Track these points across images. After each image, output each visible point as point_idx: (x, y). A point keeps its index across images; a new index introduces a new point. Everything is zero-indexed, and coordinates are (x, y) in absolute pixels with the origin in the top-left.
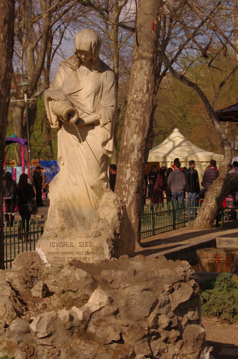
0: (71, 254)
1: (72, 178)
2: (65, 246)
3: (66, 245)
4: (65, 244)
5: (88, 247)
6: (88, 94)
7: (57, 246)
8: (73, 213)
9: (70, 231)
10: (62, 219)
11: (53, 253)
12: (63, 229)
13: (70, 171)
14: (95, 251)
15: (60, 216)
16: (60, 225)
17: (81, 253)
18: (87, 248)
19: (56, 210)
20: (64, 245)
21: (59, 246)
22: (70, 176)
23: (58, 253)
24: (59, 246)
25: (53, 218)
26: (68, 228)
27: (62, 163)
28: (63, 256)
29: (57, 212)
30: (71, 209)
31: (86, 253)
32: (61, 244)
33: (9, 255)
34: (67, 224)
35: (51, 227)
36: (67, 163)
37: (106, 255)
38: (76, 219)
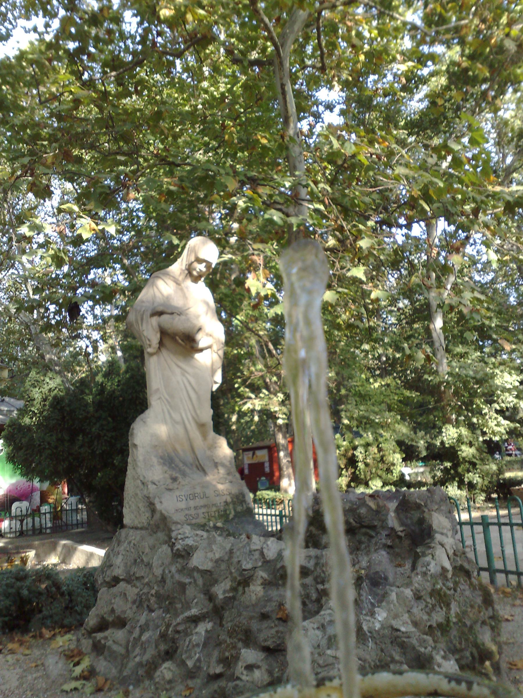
1: (173, 415)
11: (182, 510)
12: (174, 479)
13: (171, 406)
16: (167, 476)
19: (153, 457)
22: (170, 414)
23: (189, 509)
29: (155, 460)
30: (173, 454)
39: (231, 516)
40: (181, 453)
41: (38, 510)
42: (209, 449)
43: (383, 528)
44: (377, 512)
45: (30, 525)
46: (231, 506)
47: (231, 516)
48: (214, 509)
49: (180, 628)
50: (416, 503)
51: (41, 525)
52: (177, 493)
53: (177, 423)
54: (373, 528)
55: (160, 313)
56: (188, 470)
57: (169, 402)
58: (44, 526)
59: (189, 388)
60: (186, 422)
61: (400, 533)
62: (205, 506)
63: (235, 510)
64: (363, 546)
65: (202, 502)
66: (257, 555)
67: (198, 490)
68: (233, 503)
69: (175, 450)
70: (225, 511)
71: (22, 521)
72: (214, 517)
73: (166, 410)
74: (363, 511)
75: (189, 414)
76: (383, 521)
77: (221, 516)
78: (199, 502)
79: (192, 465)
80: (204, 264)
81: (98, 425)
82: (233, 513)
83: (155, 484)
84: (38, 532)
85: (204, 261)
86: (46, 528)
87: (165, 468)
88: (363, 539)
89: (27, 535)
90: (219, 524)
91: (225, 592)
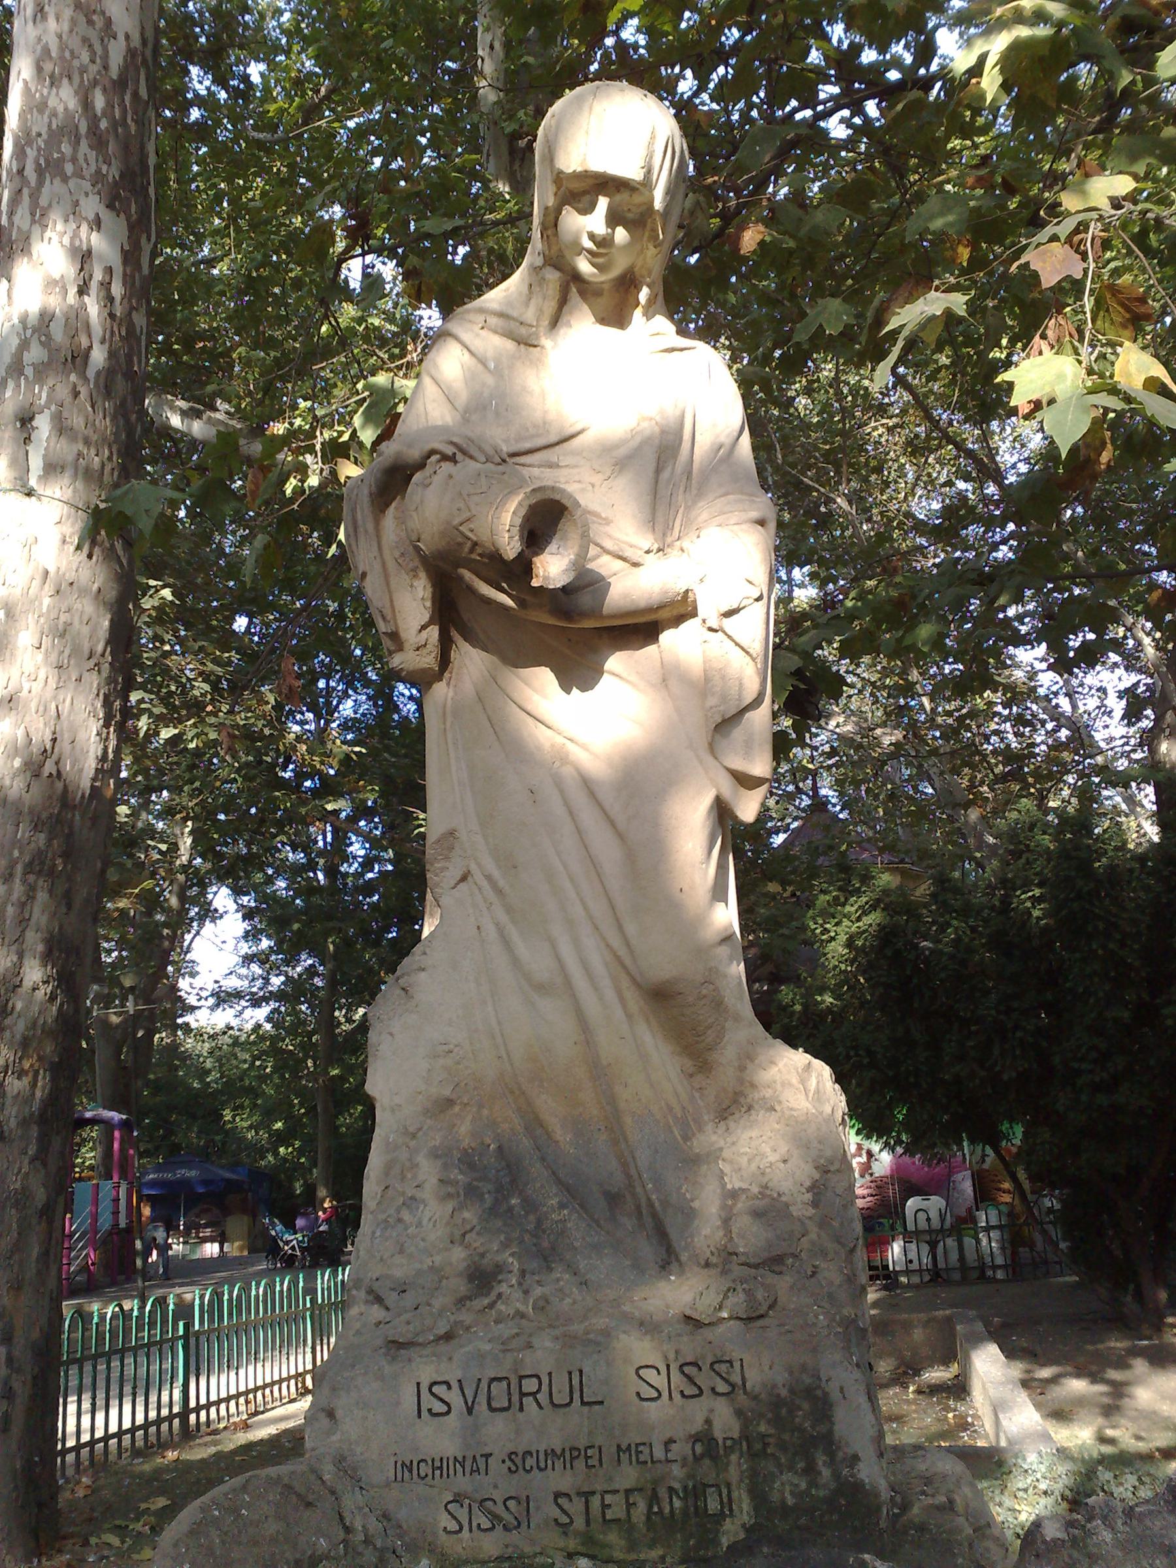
0: (580, 1464)
1: (523, 950)
2: (528, 1401)
3: (534, 1394)
4: (530, 1385)
5: (706, 1401)
7: (470, 1411)
8: (537, 1170)
9: (538, 1291)
10: (467, 1215)
11: (439, 1466)
13: (509, 910)
14: (763, 1428)
15: (449, 1196)
16: (458, 1255)
17: (659, 1453)
18: (698, 1411)
20: (522, 1395)
21: (482, 1407)
23: (476, 1463)
24: (482, 1407)
25: (406, 1216)
26: (523, 1273)
27: (455, 873)
29: (428, 1172)
31: (699, 1448)
32: (498, 1389)
34: (505, 1245)
35: (398, 1273)
36: (491, 866)
37: (856, 1458)
38: (562, 1206)
39: (731, 1532)
40: (563, 1136)
45: (954, 1256)
46: (736, 1468)
47: (731, 1532)
48: (628, 1476)
51: (980, 1257)
53: (541, 988)
57: (499, 892)
62: (571, 1455)
63: (759, 1497)
69: (534, 1124)
70: (695, 1492)
71: (933, 1245)
73: (491, 932)
75: (590, 942)
79: (613, 1199)
83: (379, 1300)
84: (975, 1274)
86: (995, 1268)
89: (948, 1282)
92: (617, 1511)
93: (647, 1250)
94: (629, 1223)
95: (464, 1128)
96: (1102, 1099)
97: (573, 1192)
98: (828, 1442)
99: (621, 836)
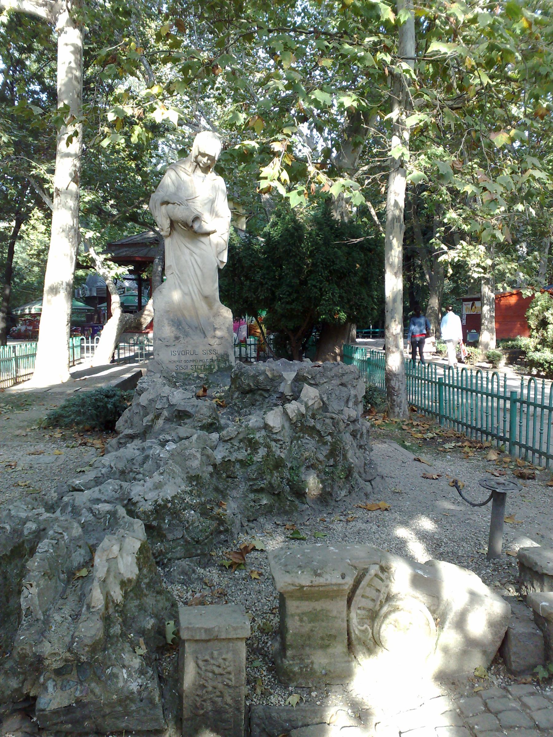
6: (206, 202)
12: (177, 338)
16: (173, 335)
23: (180, 361)
28: (186, 364)
29: (166, 322)
30: (182, 319)
33: (252, 350)
39: (215, 370)
40: (188, 318)
41: (245, 341)
42: (214, 316)
43: (275, 392)
44: (272, 380)
46: (216, 363)
48: (201, 364)
49: (122, 441)
50: (303, 376)
51: (247, 354)
52: (172, 349)
54: (267, 391)
55: (167, 203)
56: (191, 332)
58: (249, 356)
59: (196, 266)
60: (193, 294)
61: (288, 397)
63: (218, 366)
64: (258, 403)
65: (192, 358)
66: (165, 400)
67: (189, 348)
68: (218, 360)
69: (183, 315)
70: (210, 366)
72: (201, 369)
74: (261, 378)
75: (195, 288)
76: (276, 387)
77: (205, 369)
78: (189, 357)
79: (196, 328)
80: (207, 158)
81: (260, 274)
82: (217, 368)
84: (244, 360)
85: (207, 155)
86: (251, 358)
87: (173, 329)
88: (258, 397)
90: (202, 375)
91: (148, 421)
92: (199, 367)
93: (202, 336)
94: (198, 331)
95: (171, 315)
96: (288, 307)
97: (190, 326)
98: (228, 360)
99: (201, 270)
